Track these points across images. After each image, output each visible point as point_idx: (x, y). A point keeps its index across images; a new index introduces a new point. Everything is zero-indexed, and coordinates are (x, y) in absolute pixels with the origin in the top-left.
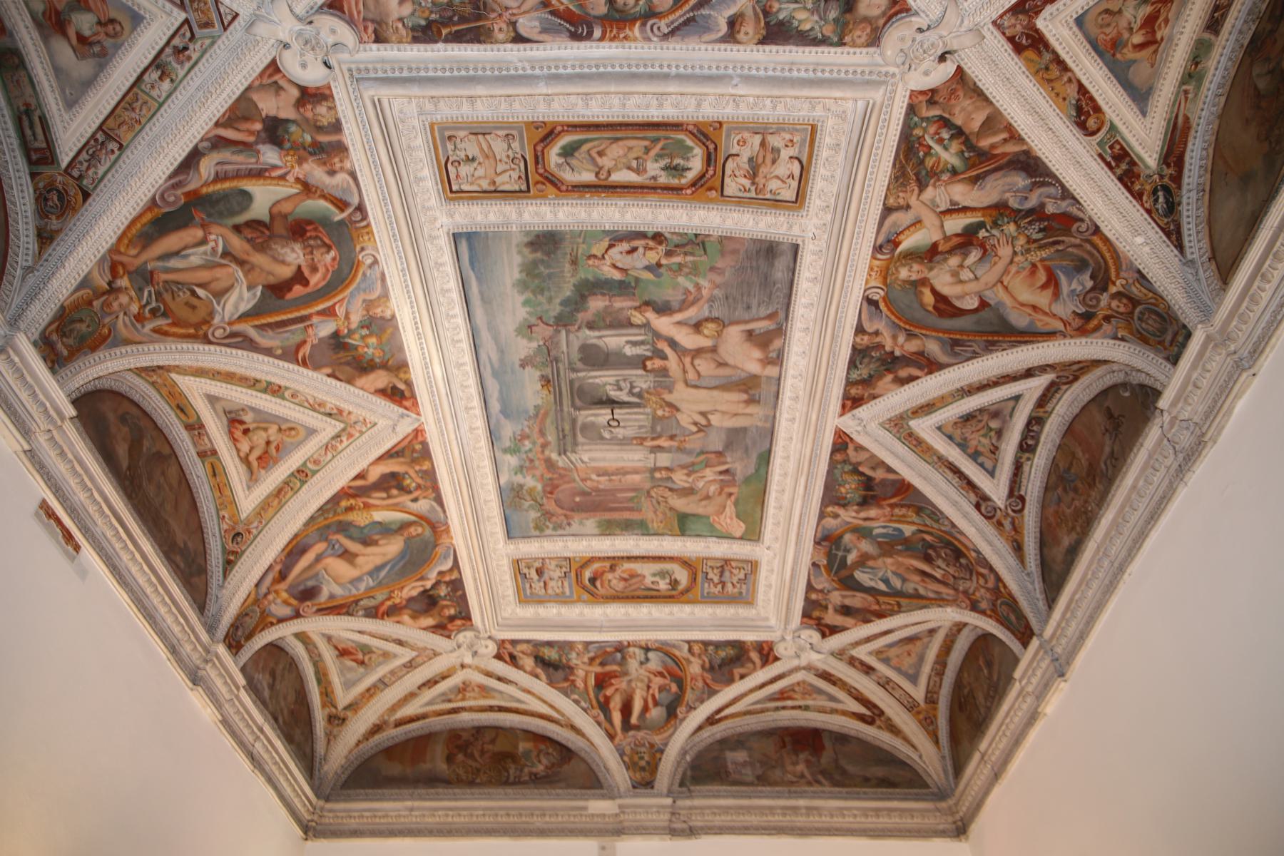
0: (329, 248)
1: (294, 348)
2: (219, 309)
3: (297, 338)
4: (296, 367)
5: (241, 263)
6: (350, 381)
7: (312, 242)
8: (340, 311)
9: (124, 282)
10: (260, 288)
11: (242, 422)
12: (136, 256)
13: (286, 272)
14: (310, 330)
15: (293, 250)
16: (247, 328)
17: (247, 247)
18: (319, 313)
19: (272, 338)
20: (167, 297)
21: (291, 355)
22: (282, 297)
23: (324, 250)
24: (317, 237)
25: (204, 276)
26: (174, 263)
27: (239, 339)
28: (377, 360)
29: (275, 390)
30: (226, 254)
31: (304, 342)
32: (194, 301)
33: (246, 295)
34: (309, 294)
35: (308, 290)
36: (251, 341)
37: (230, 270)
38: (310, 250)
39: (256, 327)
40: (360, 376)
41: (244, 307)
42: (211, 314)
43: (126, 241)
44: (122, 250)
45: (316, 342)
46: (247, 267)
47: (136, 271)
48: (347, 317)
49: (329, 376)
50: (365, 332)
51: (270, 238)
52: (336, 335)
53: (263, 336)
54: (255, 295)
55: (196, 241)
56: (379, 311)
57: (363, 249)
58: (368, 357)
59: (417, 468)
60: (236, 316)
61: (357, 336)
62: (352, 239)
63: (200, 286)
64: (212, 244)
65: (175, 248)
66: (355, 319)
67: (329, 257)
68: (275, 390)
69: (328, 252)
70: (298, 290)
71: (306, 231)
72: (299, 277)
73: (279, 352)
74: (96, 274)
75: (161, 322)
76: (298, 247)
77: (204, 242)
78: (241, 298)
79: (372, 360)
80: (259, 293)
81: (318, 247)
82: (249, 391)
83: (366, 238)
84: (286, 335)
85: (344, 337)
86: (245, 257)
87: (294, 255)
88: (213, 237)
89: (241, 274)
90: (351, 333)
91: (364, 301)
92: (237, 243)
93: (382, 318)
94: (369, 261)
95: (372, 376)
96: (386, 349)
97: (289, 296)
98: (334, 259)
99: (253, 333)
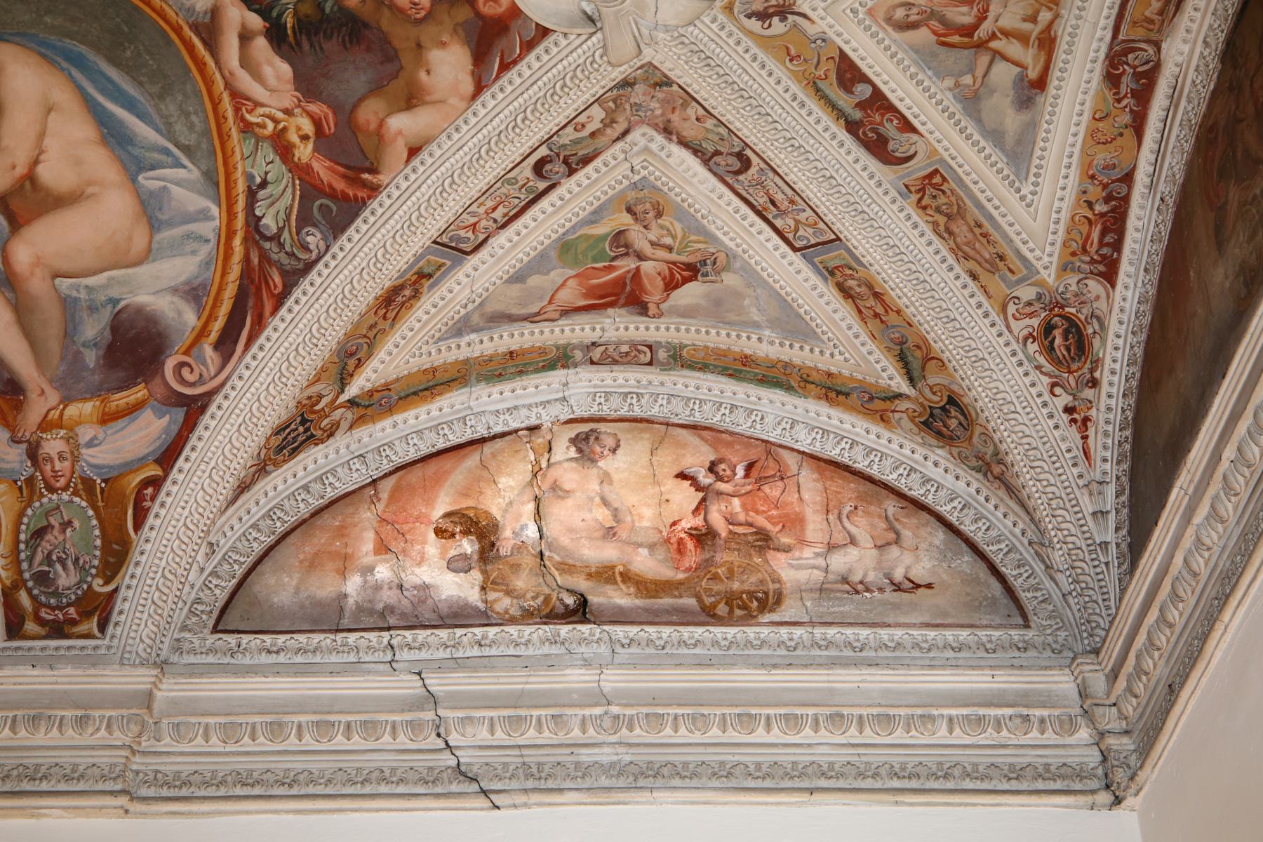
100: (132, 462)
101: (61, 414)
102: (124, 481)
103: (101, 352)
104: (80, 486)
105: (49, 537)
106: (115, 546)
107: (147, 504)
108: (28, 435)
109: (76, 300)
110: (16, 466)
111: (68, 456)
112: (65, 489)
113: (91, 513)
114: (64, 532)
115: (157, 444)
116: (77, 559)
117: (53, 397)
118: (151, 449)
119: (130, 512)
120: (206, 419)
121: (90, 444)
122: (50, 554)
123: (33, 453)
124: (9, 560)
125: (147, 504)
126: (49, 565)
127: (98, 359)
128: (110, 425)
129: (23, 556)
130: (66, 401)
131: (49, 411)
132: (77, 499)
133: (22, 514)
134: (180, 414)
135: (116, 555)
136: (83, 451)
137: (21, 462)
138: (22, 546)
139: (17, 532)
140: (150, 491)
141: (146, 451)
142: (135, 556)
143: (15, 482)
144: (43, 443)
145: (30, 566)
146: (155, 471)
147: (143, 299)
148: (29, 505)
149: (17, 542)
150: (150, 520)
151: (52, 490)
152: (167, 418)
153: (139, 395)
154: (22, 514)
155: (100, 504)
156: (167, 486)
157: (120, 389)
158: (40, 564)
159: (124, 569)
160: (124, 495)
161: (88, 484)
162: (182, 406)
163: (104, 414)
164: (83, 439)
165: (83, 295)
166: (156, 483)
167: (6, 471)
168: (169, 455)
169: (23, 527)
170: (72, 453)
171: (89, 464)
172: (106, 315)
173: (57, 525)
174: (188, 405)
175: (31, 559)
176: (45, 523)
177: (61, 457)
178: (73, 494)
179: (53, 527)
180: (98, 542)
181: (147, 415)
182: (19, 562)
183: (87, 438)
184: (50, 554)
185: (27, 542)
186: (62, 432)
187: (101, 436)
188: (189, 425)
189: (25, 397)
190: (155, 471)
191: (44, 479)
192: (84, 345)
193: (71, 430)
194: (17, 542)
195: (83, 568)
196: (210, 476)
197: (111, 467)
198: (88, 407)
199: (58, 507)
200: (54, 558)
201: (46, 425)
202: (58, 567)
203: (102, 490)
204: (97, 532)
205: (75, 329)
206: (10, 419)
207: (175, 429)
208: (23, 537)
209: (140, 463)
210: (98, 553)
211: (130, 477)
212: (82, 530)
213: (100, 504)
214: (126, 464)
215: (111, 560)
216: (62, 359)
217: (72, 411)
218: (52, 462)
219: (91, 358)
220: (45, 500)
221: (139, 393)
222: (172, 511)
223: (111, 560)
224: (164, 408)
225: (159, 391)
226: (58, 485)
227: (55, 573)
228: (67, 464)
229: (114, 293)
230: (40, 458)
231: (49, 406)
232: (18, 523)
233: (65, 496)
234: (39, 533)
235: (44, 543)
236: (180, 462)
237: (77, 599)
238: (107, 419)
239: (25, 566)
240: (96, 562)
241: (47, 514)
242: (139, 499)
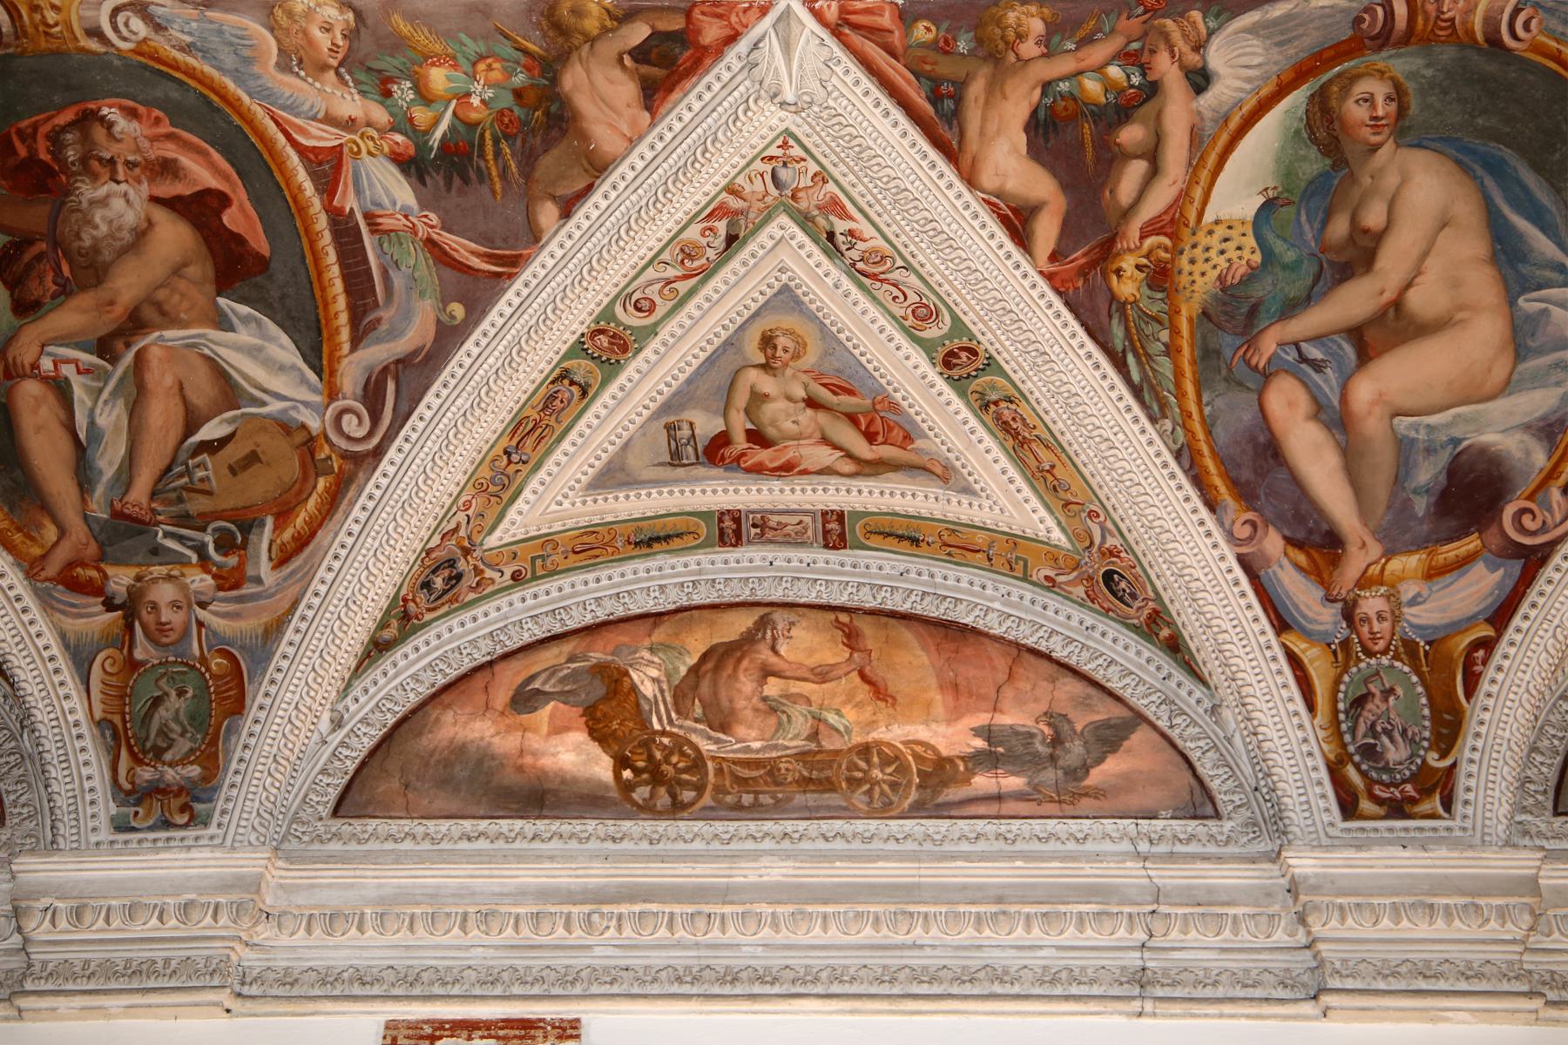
0: (88, 119)
1: (448, 273)
2: (274, 407)
3: (415, 260)
4: (518, 284)
5: (135, 324)
6: (598, 167)
7: (71, 154)
8: (322, 137)
9: (120, 579)
10: (222, 301)
11: (722, 439)
12: (62, 532)
13: (173, 237)
14: (387, 223)
15: (104, 202)
16: (353, 368)
17: (85, 300)
18: (328, 184)
19: (407, 316)
20: (198, 504)
21: (473, 291)
22: (263, 264)
23: (99, 133)
24: (55, 138)
25: (162, 414)
26: (108, 461)
27: (391, 386)
28: (520, 79)
29: (609, 345)
30: (105, 348)
31: (430, 243)
32: (233, 453)
33: (244, 336)
34: (256, 200)
35: (240, 195)
36: (403, 362)
37: (155, 353)
38: (96, 165)
39: (356, 343)
40: (584, 137)
41: (284, 349)
42: (286, 427)
43: (18, 537)
44: (36, 551)
45: (434, 219)
46: (149, 313)
47: (101, 546)
48: (350, 124)
49: (566, 213)
50: (404, 92)
51: (56, 244)
52: (412, 165)
53: (394, 334)
54: (246, 320)
55: (51, 398)
56: (323, 40)
57: (95, 33)
58: (507, 100)
59: (1029, 49)
60: (312, 376)
61: (421, 115)
62: (56, 53)
63: (191, 427)
64: (68, 370)
65: (65, 446)
66: (350, 104)
67: (122, 124)
68: (609, 345)
69: (110, 125)
70: (240, 218)
71: (33, 159)
72: (200, 210)
73: (458, 310)
74: (74, 625)
75: (264, 539)
76: (87, 191)
77: (62, 390)
78: (253, 352)
79: (518, 94)
80: (244, 309)
81: (86, 138)
82: (597, 407)
83: (51, 17)
84: (398, 280)
85: (422, 147)
86: (119, 310)
87: (118, 204)
88: (47, 364)
89: (169, 334)
90: (403, 124)
91: (284, 66)
92: (71, 316)
93: (352, 35)
94: (137, 25)
95: (584, 104)
96: (472, 47)
97: (260, 242)
98: (132, 114)
99: (377, 353)
100: (1460, 621)
101: (1383, 569)
102: (1451, 643)
103: (1433, 499)
104: (1401, 650)
105: (1370, 706)
106: (1447, 717)
107: (1478, 668)
108: (1344, 592)
109: (1413, 441)
110: (1329, 627)
111: (1388, 615)
112: (1385, 652)
113: (1415, 679)
114: (1387, 701)
115: (1489, 600)
116: (1404, 733)
117: (1375, 550)
118: (1482, 606)
119: (1459, 678)
120: (1548, 572)
121: (1413, 602)
122: (1373, 725)
123: (1349, 614)
124: (1329, 732)
125: (1478, 668)
126: (1375, 737)
127: (1428, 507)
128: (1436, 579)
129: (1344, 727)
130: (1389, 554)
131: (1369, 566)
132: (1397, 664)
133: (1338, 681)
134: (1516, 567)
135: (1448, 727)
136: (1405, 610)
137: (1336, 623)
138: (1342, 717)
139: (1335, 701)
140: (1481, 653)
141: (1476, 609)
142: (1471, 726)
143: (1329, 645)
144: (1361, 602)
145: (1354, 738)
146: (1487, 631)
147: (1489, 438)
148: (1346, 670)
149: (1336, 712)
150: (1485, 686)
151: (1370, 653)
152: (1501, 571)
153: (1472, 546)
154: (1338, 681)
155: (1425, 669)
156: (1502, 647)
157: (1450, 540)
158: (1365, 736)
159: (1459, 741)
160: (1451, 659)
161: (1410, 647)
162: (1519, 558)
163: (1431, 567)
164: (1405, 597)
165: (1422, 436)
166: (1488, 645)
167: (1320, 633)
168: (1502, 614)
169: (1341, 695)
170: (1393, 612)
171: (1411, 625)
172: (1444, 458)
173: (1378, 693)
174: (1526, 557)
175: (1353, 730)
176: (1364, 691)
177: (1380, 617)
178: (1393, 658)
179: (1373, 695)
180: (1426, 712)
181: (1479, 568)
182: (1340, 735)
183: (1410, 595)
184: (1373, 725)
185: (1346, 712)
186: (1383, 590)
187: (1425, 593)
188: (1527, 579)
189: (1344, 550)
190: (1487, 631)
191: (1360, 642)
192: (1415, 492)
193: (1393, 586)
194: (1336, 712)
195: (1412, 741)
196: (1554, 636)
197: (1436, 628)
198: (1413, 561)
199: (1377, 673)
200: (1379, 729)
201: (1364, 582)
202: (1385, 740)
203: (1426, 653)
204: (1424, 701)
205: (1407, 473)
206: (1325, 576)
207: (1510, 584)
208: (1341, 706)
209: (1469, 622)
210: (1427, 723)
211: (1457, 639)
212: (1406, 701)
213: (1425, 669)
214: (1453, 624)
215: (1444, 731)
216: (1389, 507)
217: (1396, 565)
218: (1370, 623)
219: (1421, 505)
220: (1362, 665)
221: (1471, 543)
222: (1511, 675)
223: (1444, 731)
224: (1499, 560)
225: (1494, 539)
226: (1377, 648)
227: (1383, 745)
228: (1387, 625)
229: (1457, 432)
230: (1357, 619)
231: (1369, 560)
232: (1335, 691)
233: (1385, 661)
234: (1359, 702)
235: (1365, 713)
236: (1517, 621)
237: (1413, 775)
238: (1433, 573)
239: (1348, 738)
240: (1427, 734)
241: (1366, 681)
242: (1469, 663)
